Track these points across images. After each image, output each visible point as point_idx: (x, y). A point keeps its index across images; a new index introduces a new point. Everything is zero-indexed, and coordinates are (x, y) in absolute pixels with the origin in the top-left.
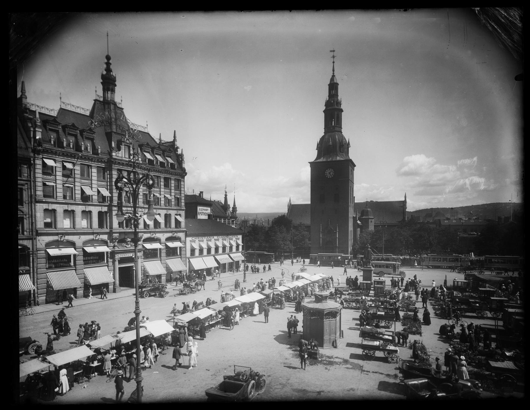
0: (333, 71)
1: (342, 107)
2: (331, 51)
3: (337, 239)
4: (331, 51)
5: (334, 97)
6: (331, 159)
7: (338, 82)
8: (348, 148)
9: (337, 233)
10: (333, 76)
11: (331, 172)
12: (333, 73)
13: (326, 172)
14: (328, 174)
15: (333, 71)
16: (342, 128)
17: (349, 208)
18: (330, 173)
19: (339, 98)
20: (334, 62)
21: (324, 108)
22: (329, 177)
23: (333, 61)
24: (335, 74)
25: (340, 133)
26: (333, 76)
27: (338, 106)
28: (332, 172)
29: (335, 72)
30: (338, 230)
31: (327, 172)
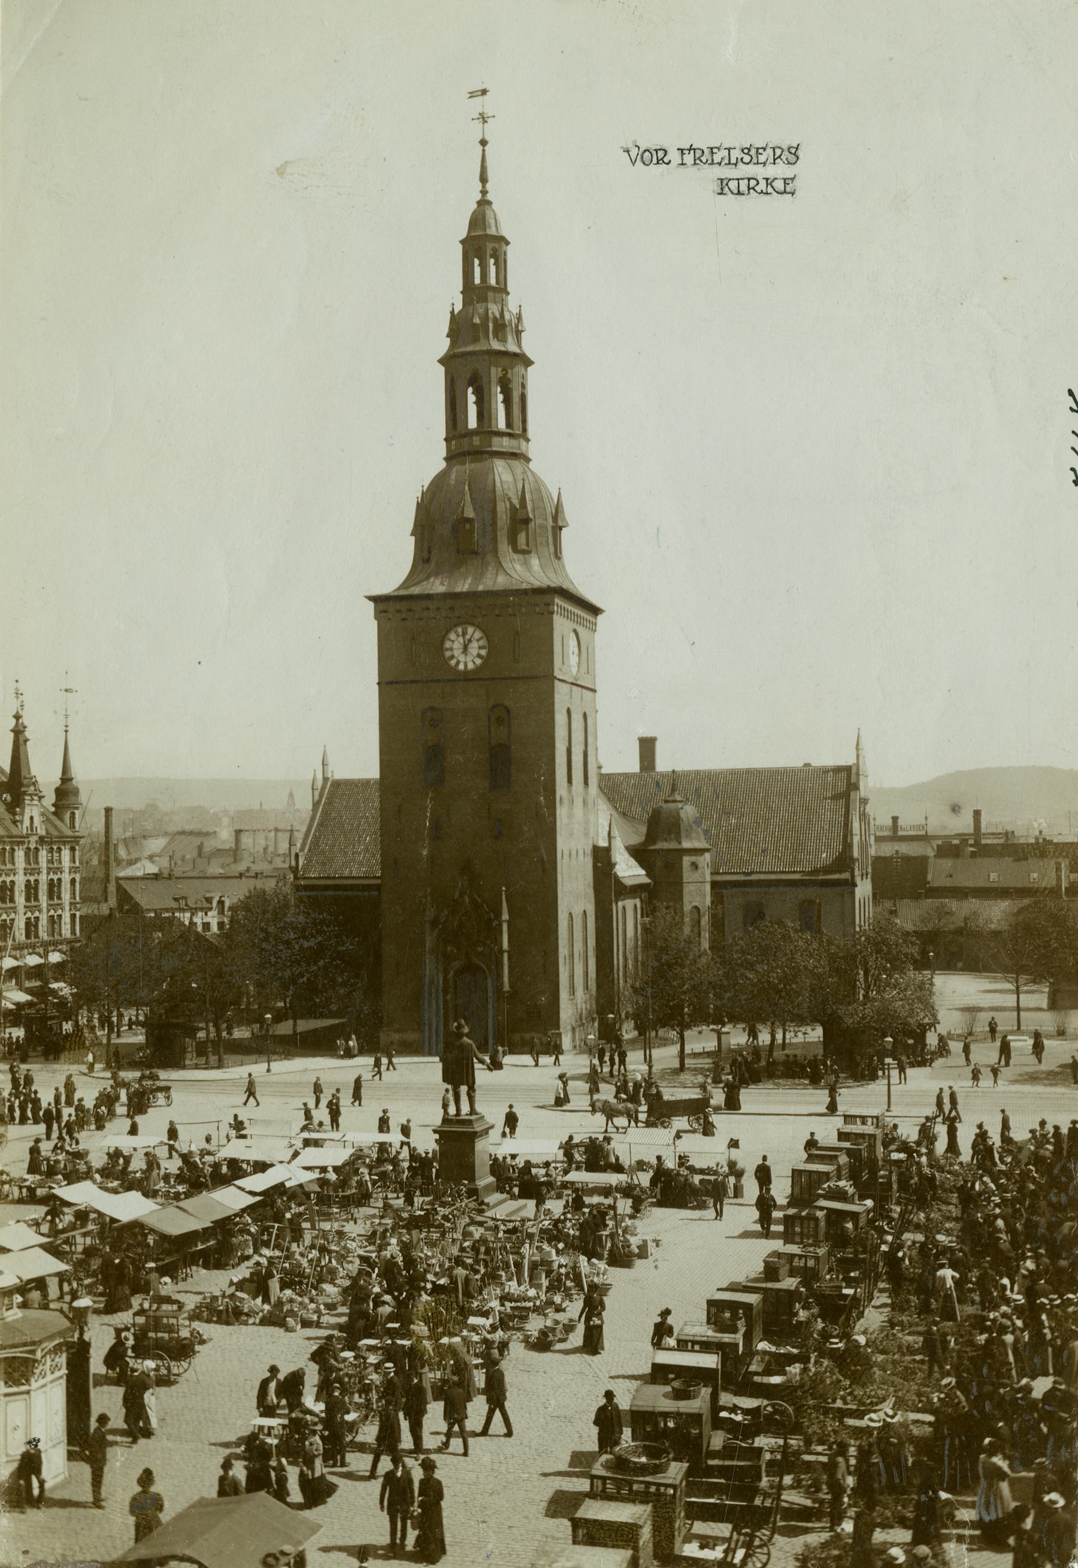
0: (484, 179)
1: (529, 346)
2: (472, 95)
3: (506, 956)
4: (472, 95)
5: (486, 300)
6: (469, 581)
7: (504, 232)
8: (557, 529)
9: (505, 927)
10: (484, 203)
11: (470, 641)
12: (484, 192)
13: (448, 644)
14: (456, 653)
15: (484, 179)
16: (528, 440)
17: (561, 812)
18: (465, 649)
19: (512, 304)
20: (484, 143)
21: (443, 345)
22: (461, 667)
23: (480, 137)
24: (489, 197)
25: (516, 464)
26: (484, 203)
27: (504, 340)
28: (474, 645)
29: (488, 186)
30: (505, 916)
31: (454, 643)
